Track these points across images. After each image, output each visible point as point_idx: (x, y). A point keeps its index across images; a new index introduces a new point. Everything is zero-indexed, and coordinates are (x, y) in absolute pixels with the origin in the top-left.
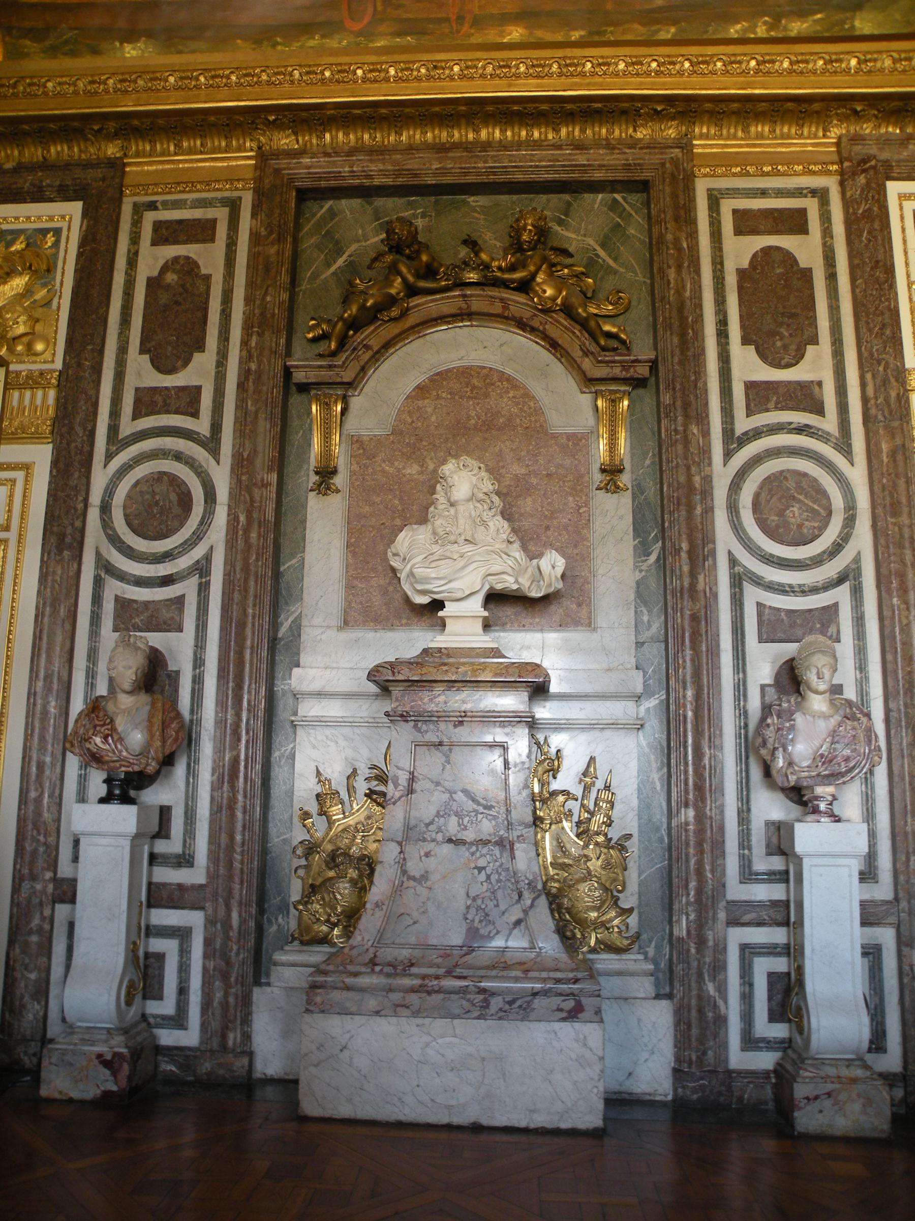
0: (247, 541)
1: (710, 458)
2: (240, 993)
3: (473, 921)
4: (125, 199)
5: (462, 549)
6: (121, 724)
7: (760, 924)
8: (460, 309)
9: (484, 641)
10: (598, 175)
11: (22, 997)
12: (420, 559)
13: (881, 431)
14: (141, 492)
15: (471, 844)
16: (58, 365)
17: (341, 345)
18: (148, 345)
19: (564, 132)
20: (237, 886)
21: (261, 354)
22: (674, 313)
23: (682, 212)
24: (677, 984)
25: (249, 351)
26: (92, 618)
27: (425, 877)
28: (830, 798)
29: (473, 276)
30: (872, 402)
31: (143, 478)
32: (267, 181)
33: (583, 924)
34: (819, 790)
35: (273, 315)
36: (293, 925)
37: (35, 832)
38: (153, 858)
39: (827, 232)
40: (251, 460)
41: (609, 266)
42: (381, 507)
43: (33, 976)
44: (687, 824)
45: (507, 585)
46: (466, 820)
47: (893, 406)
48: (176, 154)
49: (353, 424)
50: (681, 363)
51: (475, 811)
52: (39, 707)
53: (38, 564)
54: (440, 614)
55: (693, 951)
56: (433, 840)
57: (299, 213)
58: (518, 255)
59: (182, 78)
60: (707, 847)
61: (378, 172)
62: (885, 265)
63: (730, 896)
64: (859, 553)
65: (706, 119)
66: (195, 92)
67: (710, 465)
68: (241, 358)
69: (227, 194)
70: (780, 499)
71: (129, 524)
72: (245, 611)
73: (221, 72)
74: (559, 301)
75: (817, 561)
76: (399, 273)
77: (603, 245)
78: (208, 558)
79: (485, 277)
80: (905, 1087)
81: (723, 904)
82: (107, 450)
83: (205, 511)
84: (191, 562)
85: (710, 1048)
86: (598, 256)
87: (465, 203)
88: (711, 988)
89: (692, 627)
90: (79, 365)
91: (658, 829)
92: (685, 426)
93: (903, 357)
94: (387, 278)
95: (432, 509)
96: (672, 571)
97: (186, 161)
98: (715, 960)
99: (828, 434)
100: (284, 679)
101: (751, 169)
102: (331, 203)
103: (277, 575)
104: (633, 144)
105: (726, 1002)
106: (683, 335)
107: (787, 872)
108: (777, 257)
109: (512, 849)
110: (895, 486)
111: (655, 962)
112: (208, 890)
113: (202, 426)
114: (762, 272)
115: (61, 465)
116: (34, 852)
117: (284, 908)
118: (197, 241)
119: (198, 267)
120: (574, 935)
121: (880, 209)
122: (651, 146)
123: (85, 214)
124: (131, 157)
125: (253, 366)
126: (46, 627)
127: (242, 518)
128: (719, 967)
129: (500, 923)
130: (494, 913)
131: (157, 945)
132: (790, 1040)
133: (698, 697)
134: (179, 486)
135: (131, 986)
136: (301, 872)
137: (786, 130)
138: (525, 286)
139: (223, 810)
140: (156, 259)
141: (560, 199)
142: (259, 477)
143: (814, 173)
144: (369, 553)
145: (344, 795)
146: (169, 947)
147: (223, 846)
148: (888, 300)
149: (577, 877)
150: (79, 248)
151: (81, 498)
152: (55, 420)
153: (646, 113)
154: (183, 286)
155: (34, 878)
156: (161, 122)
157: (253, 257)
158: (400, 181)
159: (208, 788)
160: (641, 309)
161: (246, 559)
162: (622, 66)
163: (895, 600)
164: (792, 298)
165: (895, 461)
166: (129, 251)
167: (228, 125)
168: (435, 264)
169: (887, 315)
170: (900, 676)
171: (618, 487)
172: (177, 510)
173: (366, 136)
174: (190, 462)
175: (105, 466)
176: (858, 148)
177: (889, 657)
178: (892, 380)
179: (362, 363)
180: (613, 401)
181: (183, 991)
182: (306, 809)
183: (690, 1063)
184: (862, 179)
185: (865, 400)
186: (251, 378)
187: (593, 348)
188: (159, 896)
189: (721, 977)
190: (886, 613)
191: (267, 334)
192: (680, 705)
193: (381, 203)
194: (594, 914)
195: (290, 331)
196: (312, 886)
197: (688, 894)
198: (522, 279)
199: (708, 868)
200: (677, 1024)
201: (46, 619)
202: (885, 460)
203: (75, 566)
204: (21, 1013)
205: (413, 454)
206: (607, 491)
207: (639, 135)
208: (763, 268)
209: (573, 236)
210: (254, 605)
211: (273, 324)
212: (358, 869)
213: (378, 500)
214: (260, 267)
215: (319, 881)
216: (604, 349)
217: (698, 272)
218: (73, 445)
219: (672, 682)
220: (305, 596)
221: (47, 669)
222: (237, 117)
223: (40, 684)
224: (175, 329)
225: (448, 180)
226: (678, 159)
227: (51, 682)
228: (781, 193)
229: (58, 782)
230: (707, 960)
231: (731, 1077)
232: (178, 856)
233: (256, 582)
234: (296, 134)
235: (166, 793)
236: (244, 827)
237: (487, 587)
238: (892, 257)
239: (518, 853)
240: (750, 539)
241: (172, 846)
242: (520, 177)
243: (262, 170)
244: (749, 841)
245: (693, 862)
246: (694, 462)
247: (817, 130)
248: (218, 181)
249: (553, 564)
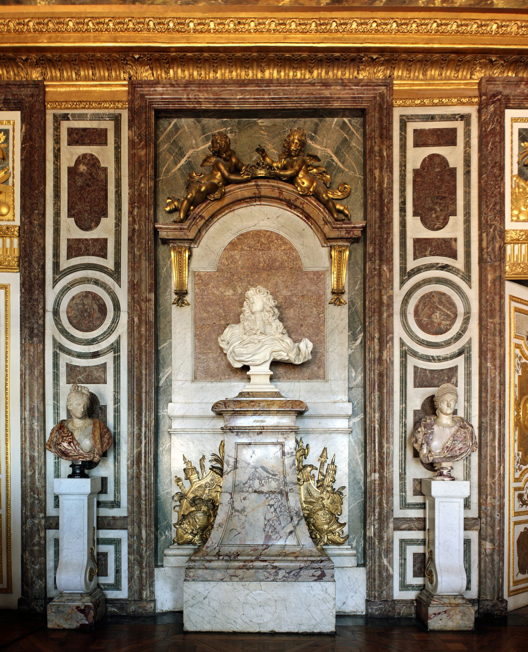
0: (139, 332)
1: (392, 285)
2: (148, 571)
3: (268, 532)
4: (47, 111)
5: (258, 337)
6: (77, 435)
7: (410, 529)
8: (255, 193)
9: (271, 388)
10: (336, 105)
11: (32, 578)
12: (236, 342)
13: (489, 268)
14: (76, 303)
15: (266, 493)
16: (18, 222)
17: (187, 216)
18: (73, 212)
19: (315, 73)
20: (144, 517)
21: (140, 220)
22: (378, 197)
23: (384, 132)
24: (368, 560)
25: (133, 218)
26: (54, 376)
27: (243, 510)
28: (450, 468)
29: (261, 173)
30: (485, 250)
31: (77, 295)
32: (136, 103)
33: (320, 531)
34: (444, 465)
35: (146, 196)
36: (174, 535)
37: (32, 493)
38: (99, 504)
39: (467, 144)
40: (139, 285)
41: (339, 168)
42: (213, 314)
43: (37, 567)
44: (375, 480)
45: (282, 357)
46: (263, 481)
47: (497, 253)
48: (77, 80)
49: (195, 265)
50: (380, 228)
51: (267, 477)
52: (28, 426)
53: (19, 345)
54: (248, 373)
55: (377, 543)
56: (247, 492)
57: (157, 127)
58: (288, 159)
59: (78, 23)
60: (384, 491)
61: (205, 99)
62: (500, 165)
63: (395, 516)
65: (401, 65)
66: (87, 34)
67: (392, 289)
68: (129, 221)
69: (112, 111)
70: (429, 308)
71: (71, 323)
72: (141, 372)
73: (102, 20)
74: (311, 190)
75: (448, 343)
76: (219, 170)
77: (336, 154)
78: (118, 342)
79: (270, 173)
80: (479, 606)
81: (391, 520)
82: (54, 278)
83: (114, 315)
84: (108, 345)
85: (384, 590)
86: (333, 160)
87: (256, 123)
88: (385, 561)
89: (379, 379)
90: (31, 223)
91: (359, 483)
92: (380, 266)
93: (504, 223)
94: (212, 173)
95: (242, 316)
96: (370, 349)
97: (84, 86)
98: (388, 547)
99: (458, 270)
100: (163, 409)
101: (426, 101)
102: (175, 120)
103: (157, 352)
104: (358, 82)
105: (393, 568)
106: (381, 211)
107: (424, 504)
108: (437, 161)
109: (287, 496)
110: (493, 299)
111: (356, 549)
112: (129, 519)
113: (109, 263)
114: (427, 171)
115: (27, 286)
116: (33, 504)
117: (168, 527)
118: (97, 144)
119: (99, 162)
120: (316, 537)
121: (500, 128)
122: (369, 84)
123: (23, 120)
124: (48, 81)
125: (136, 227)
126: (27, 381)
127: (136, 320)
128: (389, 551)
129: (281, 532)
130: (279, 528)
131: (103, 548)
132: (424, 585)
133: (381, 417)
134: (98, 300)
135: (91, 571)
136: (177, 509)
137: (448, 73)
138: (292, 180)
139: (134, 479)
140: (72, 155)
141: (312, 121)
142: (144, 296)
143: (463, 104)
144: (207, 337)
145: (199, 469)
146: (110, 549)
147: (135, 497)
148: (500, 187)
149: (317, 508)
150: (22, 144)
151: (41, 307)
152: (20, 258)
153: (366, 61)
154: (90, 174)
155: (33, 517)
156: (65, 55)
157: (132, 157)
158: (218, 107)
159: (126, 468)
160: (357, 196)
161: (140, 343)
162: (354, 25)
163: (489, 364)
164: (443, 187)
165: (495, 285)
166: (54, 148)
167: (109, 60)
168: (240, 165)
169: (498, 196)
171: (341, 303)
172: (97, 315)
173: (195, 73)
174: (103, 286)
175: (53, 288)
176: (491, 87)
177: (484, 395)
179: (199, 227)
180: (340, 252)
181: (118, 571)
182: (178, 476)
183: (375, 597)
184: (491, 108)
185: (481, 249)
186: (136, 234)
187: (330, 219)
188: (103, 523)
189: (390, 556)
190: (484, 371)
191: (143, 208)
192: (372, 421)
193: (206, 122)
194: (326, 527)
195: (156, 206)
196: (183, 515)
197: (375, 515)
198: (291, 175)
199: (384, 502)
200: (368, 579)
201: (27, 377)
203: (41, 347)
204: (32, 585)
205: (230, 283)
206: (335, 304)
207: (361, 77)
208: (428, 169)
209: (319, 147)
210: (146, 369)
211: (146, 201)
212: (207, 506)
213: (211, 310)
214: (136, 164)
215: (186, 513)
216: (336, 220)
217: (391, 172)
218: (32, 274)
219: (368, 409)
220: (173, 363)
221: (30, 405)
222: (114, 54)
223: (27, 413)
224: (88, 202)
225: (247, 107)
226: (384, 94)
227: (34, 412)
228: (443, 118)
229: (43, 467)
230: (384, 547)
231: (394, 603)
232: (112, 502)
233: (146, 356)
234: (152, 69)
235: (105, 470)
236: (146, 487)
237: (272, 358)
238: (504, 159)
239: (290, 498)
240: (412, 331)
241: (109, 497)
242: (289, 106)
243: (133, 95)
244: (405, 488)
245: (377, 499)
246: (384, 287)
247: (467, 73)
248: (106, 102)
249: (306, 346)
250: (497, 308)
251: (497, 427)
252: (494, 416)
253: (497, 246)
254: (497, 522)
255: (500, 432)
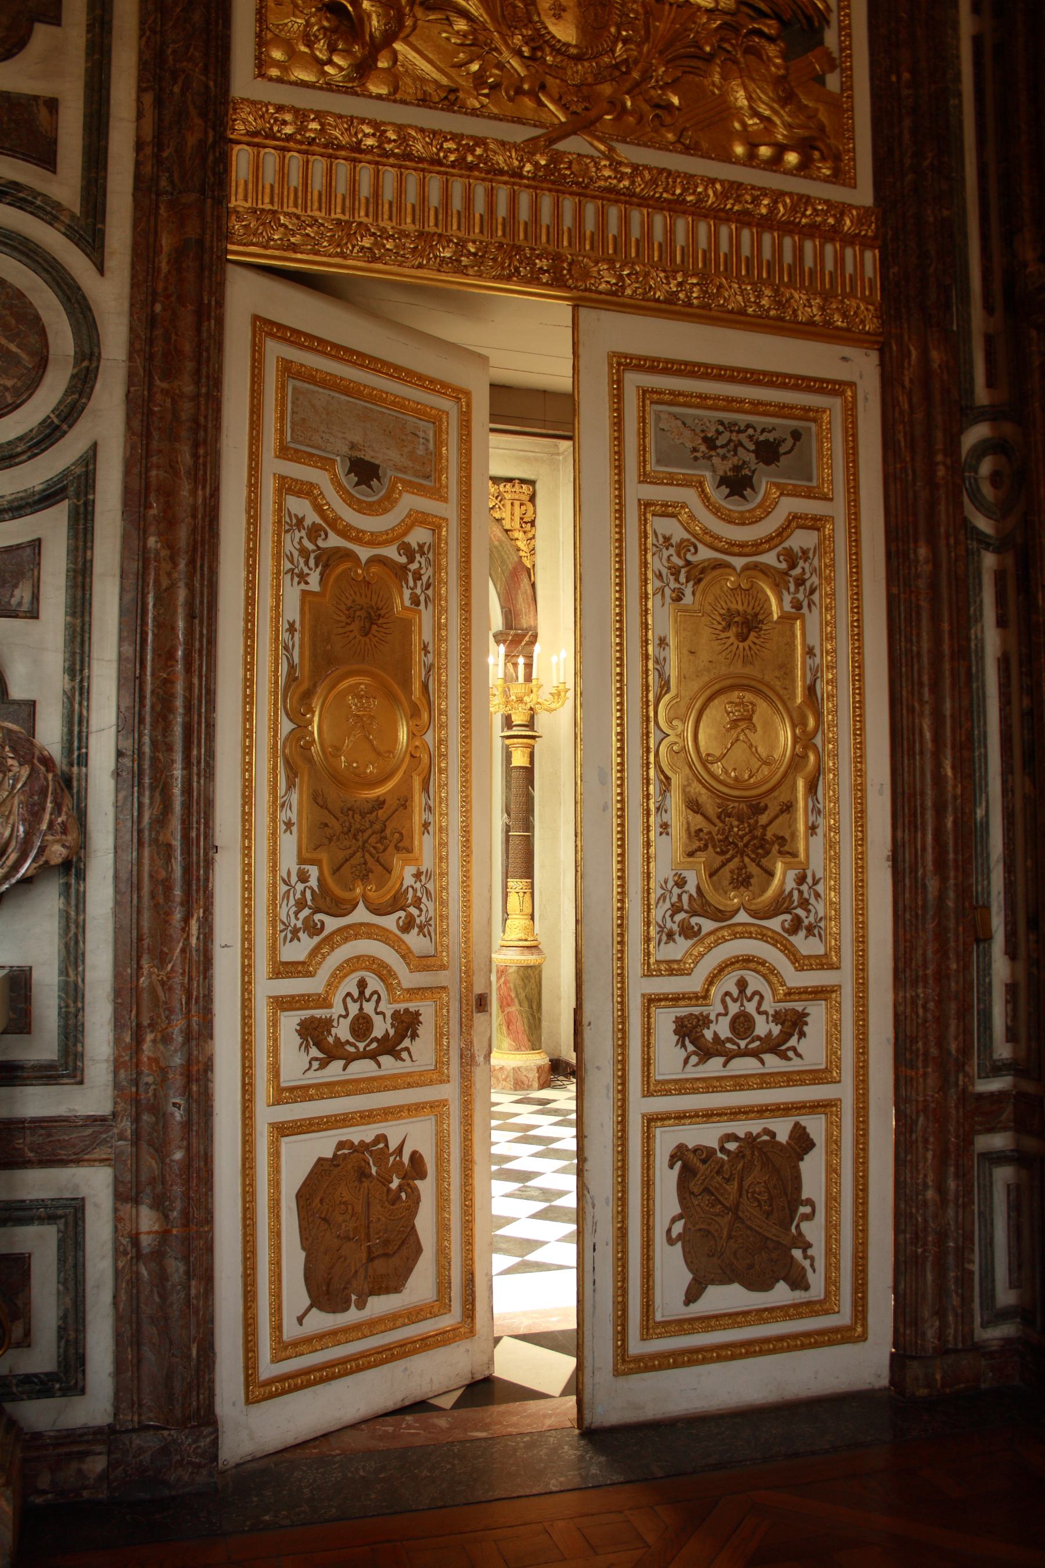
64: (94, 447)
99: (58, 205)
170: (149, 688)
178: (194, 112)
202: (164, 267)
250: (188, 348)
251: (178, 772)
252: (167, 729)
253: (192, 140)
254: (176, 1133)
255: (187, 790)
